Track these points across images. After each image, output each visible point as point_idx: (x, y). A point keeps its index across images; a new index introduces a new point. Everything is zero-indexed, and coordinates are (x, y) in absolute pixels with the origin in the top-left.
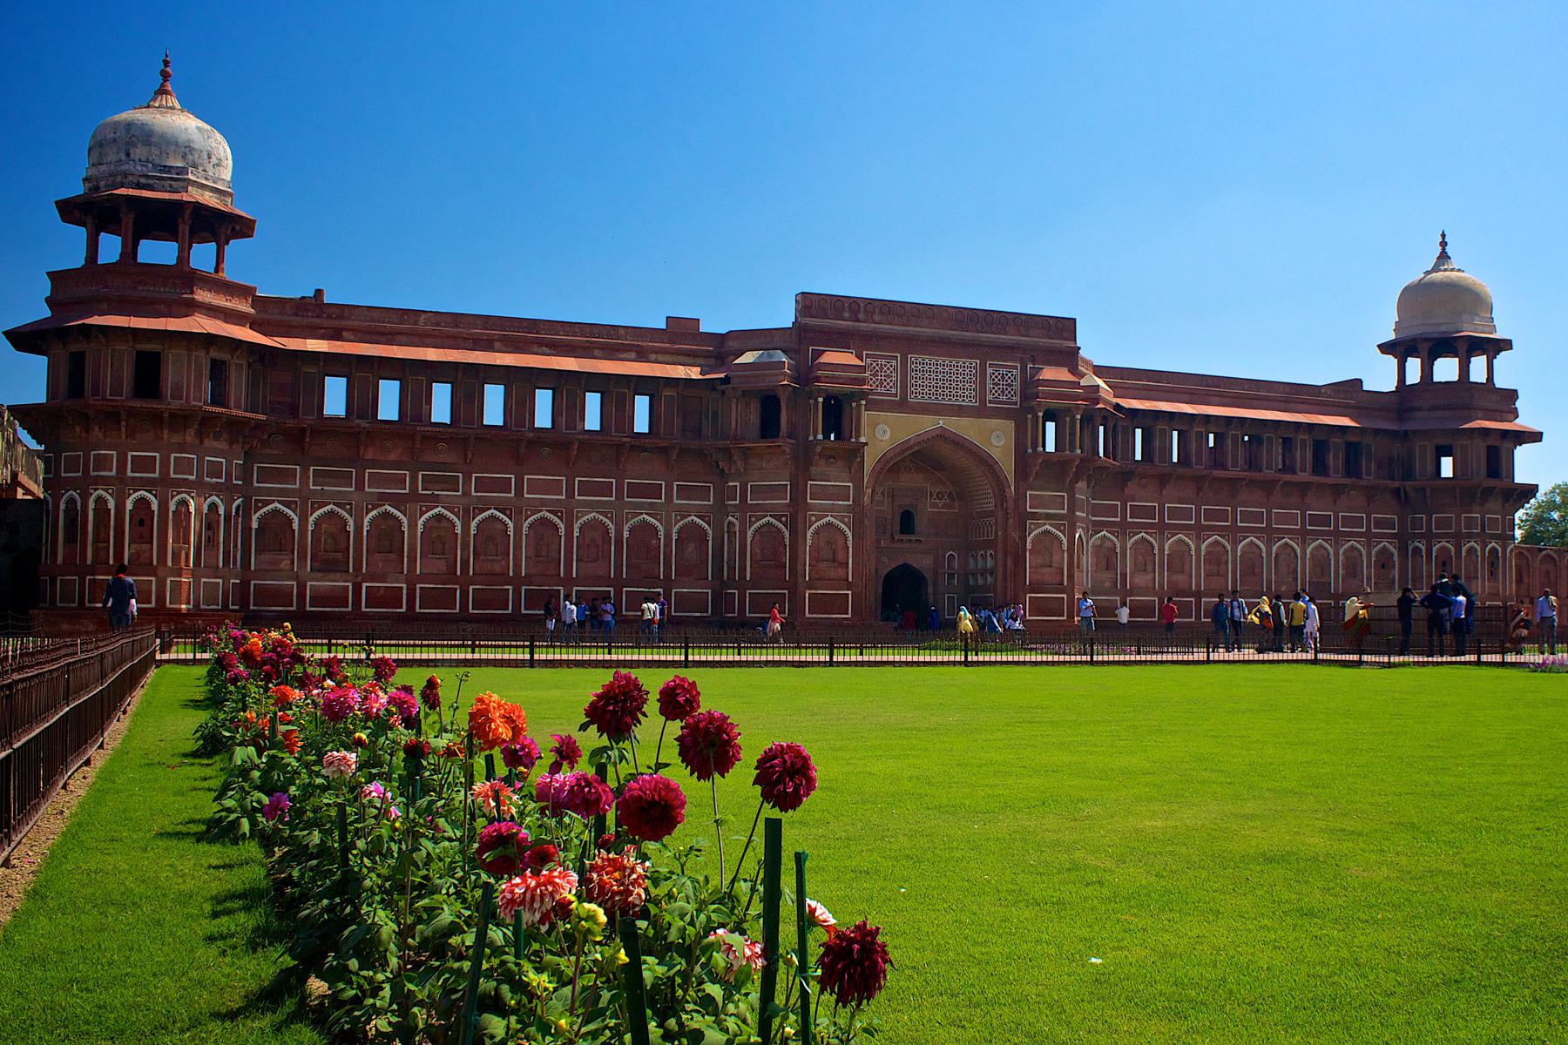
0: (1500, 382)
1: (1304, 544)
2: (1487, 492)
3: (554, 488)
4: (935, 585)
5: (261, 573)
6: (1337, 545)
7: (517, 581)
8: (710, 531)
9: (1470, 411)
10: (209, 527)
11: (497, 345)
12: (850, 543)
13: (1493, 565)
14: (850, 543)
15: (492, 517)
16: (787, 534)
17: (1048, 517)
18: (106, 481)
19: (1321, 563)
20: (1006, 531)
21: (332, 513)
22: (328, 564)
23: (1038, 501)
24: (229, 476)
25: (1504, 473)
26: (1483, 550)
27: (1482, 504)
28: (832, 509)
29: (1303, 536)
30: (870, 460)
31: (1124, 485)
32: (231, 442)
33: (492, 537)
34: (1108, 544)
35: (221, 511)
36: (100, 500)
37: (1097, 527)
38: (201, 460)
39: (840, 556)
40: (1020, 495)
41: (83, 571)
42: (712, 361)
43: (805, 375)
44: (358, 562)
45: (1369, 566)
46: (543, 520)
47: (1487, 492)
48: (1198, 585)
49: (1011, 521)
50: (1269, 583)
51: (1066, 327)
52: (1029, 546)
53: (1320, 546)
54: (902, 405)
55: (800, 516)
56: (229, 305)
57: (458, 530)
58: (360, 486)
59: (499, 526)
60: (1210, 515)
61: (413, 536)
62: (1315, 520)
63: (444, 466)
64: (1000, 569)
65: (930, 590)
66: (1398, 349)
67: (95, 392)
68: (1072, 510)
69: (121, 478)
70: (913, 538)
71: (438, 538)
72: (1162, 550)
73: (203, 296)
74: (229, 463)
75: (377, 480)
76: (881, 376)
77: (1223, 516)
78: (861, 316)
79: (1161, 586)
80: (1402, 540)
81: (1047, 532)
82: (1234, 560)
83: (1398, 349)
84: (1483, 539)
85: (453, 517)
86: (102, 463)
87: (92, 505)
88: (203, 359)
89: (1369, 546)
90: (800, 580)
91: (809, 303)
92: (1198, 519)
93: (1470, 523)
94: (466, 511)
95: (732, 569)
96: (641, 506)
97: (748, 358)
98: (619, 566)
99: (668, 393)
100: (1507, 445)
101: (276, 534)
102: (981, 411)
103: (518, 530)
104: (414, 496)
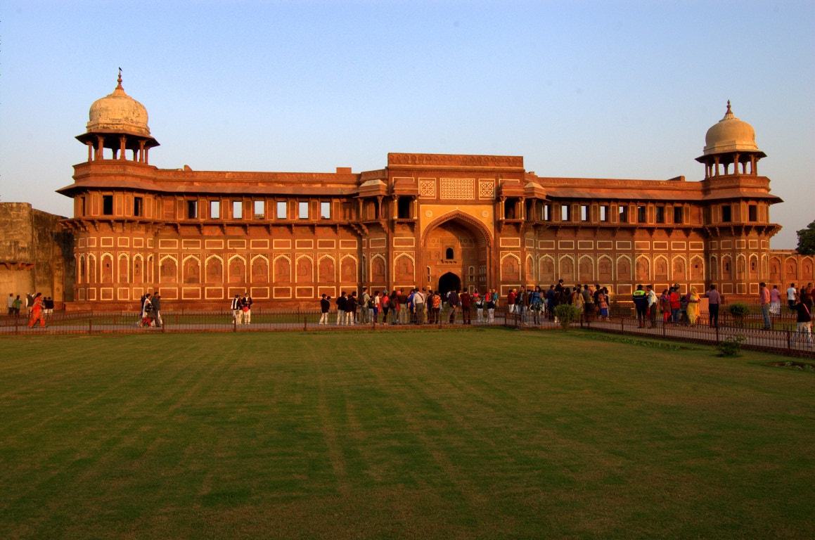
0: (760, 173)
1: (652, 256)
2: (748, 229)
3: (286, 244)
4: (464, 280)
5: (163, 285)
6: (670, 257)
7: (271, 285)
8: (356, 260)
9: (738, 187)
10: (137, 266)
11: (260, 185)
12: (414, 264)
13: (753, 264)
14: (414, 264)
15: (261, 258)
16: (385, 261)
17: (510, 249)
18: (93, 249)
19: (662, 266)
20: (490, 257)
21: (192, 259)
22: (191, 281)
23: (505, 242)
24: (145, 245)
25: (759, 217)
26: (748, 258)
27: (747, 234)
28: (405, 249)
29: (651, 253)
30: (423, 226)
31: (556, 233)
32: (147, 231)
33: (259, 266)
34: (549, 260)
35: (142, 259)
36: (90, 257)
37: (542, 253)
38: (131, 239)
39: (410, 271)
40: (496, 240)
41: (88, 286)
42: (355, 186)
43: (390, 189)
44: (203, 279)
45: (688, 266)
46: (283, 259)
47: (748, 229)
48: (596, 278)
49: (492, 252)
50: (634, 278)
51: (519, 160)
52: (501, 263)
53: (662, 258)
54: (438, 201)
55: (390, 255)
56: (142, 174)
57: (245, 263)
58: (203, 247)
59: (262, 261)
60: (601, 245)
61: (226, 267)
62: (657, 245)
63: (238, 237)
64: (488, 274)
65: (462, 283)
66: (708, 160)
67: (89, 213)
68: (523, 245)
69: (98, 248)
70: (451, 260)
71: (237, 265)
72: (576, 262)
73: (130, 170)
74: (146, 240)
75: (210, 244)
76: (427, 188)
77: (608, 245)
78: (417, 162)
79: (577, 279)
80: (707, 254)
81: (510, 256)
82: (615, 266)
83: (708, 160)
84: (747, 252)
85: (243, 259)
86: (91, 242)
87: (88, 259)
88: (131, 197)
89: (688, 256)
90: (390, 281)
91: (392, 157)
92: (595, 247)
93: (739, 244)
94: (248, 256)
95: (365, 276)
96: (326, 251)
97: (366, 184)
98: (316, 277)
99: (335, 201)
100: (761, 205)
101: (168, 268)
102: (477, 202)
103: (271, 263)
104: (226, 250)
